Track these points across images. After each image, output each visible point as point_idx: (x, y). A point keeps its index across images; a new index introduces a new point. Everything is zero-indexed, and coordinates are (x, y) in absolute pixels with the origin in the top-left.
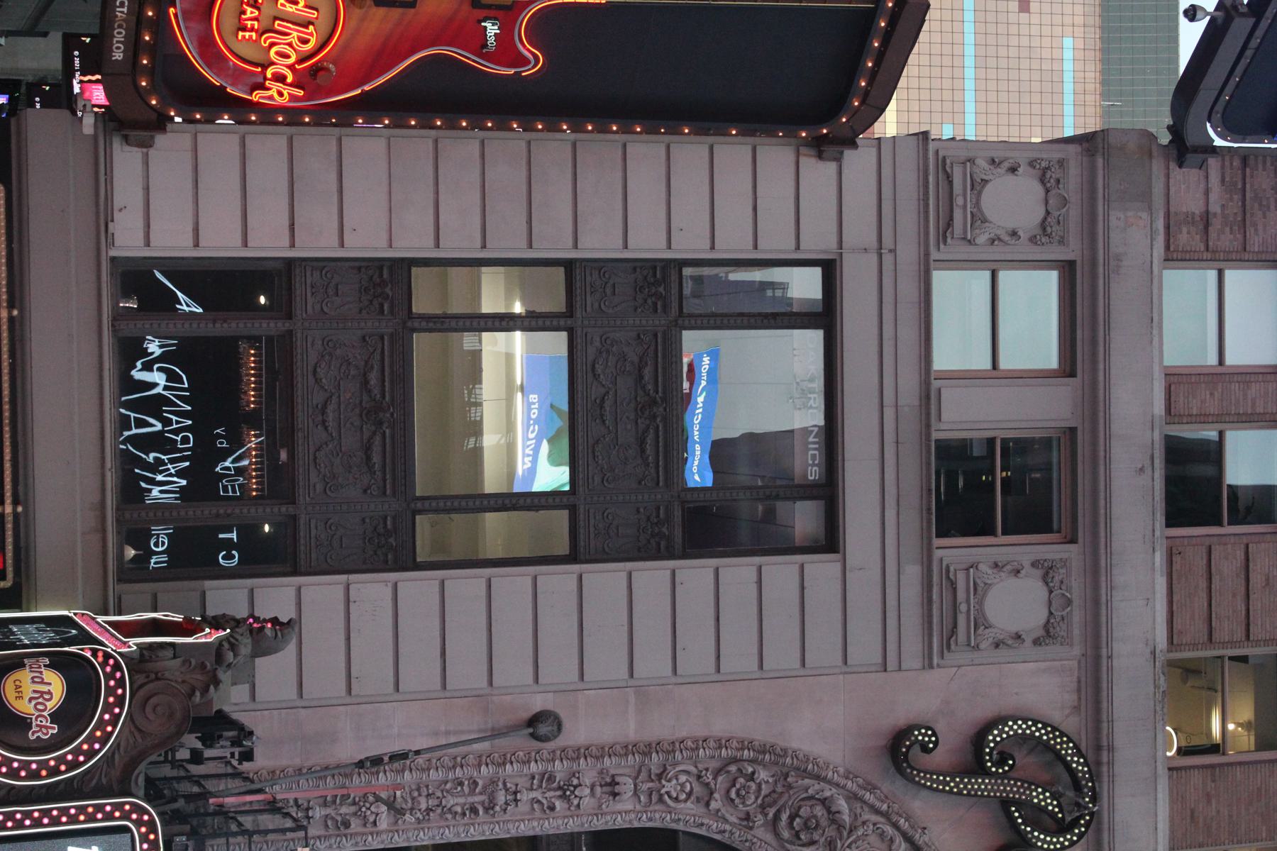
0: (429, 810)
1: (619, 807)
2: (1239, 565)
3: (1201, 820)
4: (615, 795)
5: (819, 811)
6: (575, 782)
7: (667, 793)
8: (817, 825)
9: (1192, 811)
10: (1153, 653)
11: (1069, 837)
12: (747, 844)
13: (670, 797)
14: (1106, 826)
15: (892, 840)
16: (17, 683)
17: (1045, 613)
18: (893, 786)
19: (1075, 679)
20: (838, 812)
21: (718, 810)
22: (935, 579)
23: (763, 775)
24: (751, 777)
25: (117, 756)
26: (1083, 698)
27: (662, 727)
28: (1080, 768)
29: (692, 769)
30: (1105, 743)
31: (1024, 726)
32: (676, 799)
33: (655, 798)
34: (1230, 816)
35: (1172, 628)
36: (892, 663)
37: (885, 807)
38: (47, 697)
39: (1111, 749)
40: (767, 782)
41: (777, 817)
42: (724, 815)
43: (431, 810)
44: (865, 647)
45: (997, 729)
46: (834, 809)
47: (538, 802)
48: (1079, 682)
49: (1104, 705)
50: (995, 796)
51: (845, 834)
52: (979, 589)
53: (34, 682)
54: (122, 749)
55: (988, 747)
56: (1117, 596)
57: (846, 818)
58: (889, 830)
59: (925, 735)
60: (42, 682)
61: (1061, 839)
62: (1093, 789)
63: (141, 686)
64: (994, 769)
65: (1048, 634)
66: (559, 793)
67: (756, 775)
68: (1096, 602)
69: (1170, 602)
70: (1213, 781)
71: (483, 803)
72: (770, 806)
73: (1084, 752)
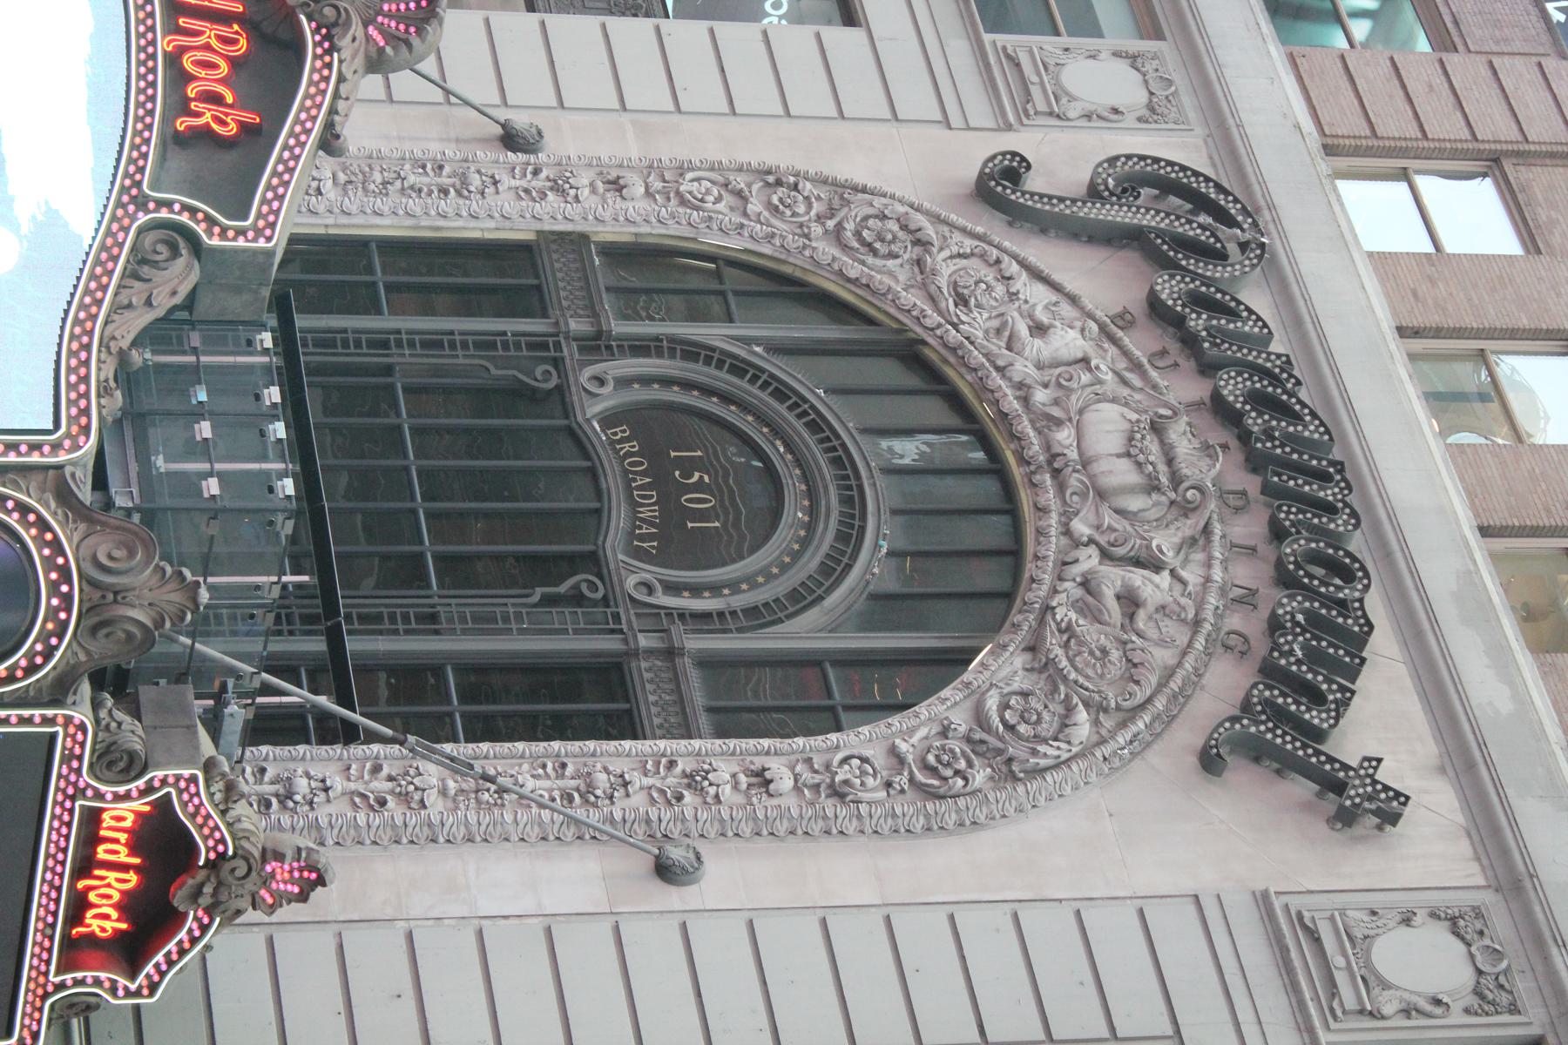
0: (385, 183)
1: (630, 205)
2: (1386, 70)
3: (1430, 301)
4: (620, 189)
5: (894, 227)
6: (568, 174)
7: (690, 193)
8: (895, 237)
10: (1298, 127)
12: (807, 253)
13: (695, 198)
14: (1291, 279)
15: (998, 261)
17: (1145, 94)
18: (989, 224)
19: (1205, 155)
20: (920, 230)
21: (759, 214)
22: (992, 59)
23: (807, 187)
24: (795, 187)
27: (669, 150)
30: (1262, 203)
32: (702, 200)
33: (674, 202)
34: (1470, 300)
35: (1319, 122)
36: (956, 120)
37: (979, 229)
39: (1272, 207)
40: (819, 198)
41: (840, 227)
42: (767, 220)
43: (388, 183)
44: (916, 98)
46: (912, 227)
47: (527, 191)
48: (1211, 158)
49: (1249, 170)
51: (935, 250)
52: (1051, 68)
56: (1229, 73)
57: (930, 231)
58: (995, 252)
65: (1152, 113)
66: (549, 184)
67: (800, 187)
68: (1207, 84)
69: (1308, 99)
70: (1433, 265)
71: (453, 186)
72: (832, 217)
73: (1226, 185)
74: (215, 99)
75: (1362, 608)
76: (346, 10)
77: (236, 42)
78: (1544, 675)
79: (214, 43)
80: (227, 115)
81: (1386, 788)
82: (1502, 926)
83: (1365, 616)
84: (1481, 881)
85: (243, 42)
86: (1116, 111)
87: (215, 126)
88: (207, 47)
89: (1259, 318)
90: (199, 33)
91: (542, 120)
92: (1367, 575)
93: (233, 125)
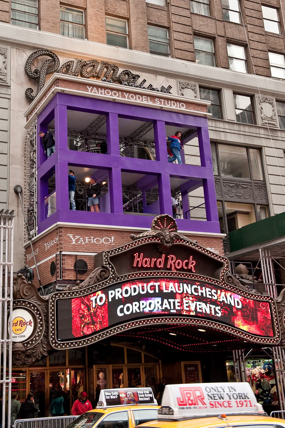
9: (51, 27)
11: (56, 59)
16: (16, 330)
25: (38, 303)
26: (20, 48)
28: (40, 53)
29: (32, 153)
31: (28, 65)
38: (21, 322)
45: (28, 72)
50: (45, 76)
53: (17, 326)
54: (37, 302)
55: (32, 75)
59: (28, 91)
60: (17, 323)
61: (57, 61)
62: (45, 51)
63: (21, 296)
64: (38, 75)
74: (187, 264)
75: (134, 75)
76: (174, 235)
77: (172, 257)
78: (136, 50)
79: (173, 262)
80: (191, 262)
81: (168, 88)
82: (182, 81)
83: (136, 75)
84: (175, 80)
85: (173, 256)
86: (4, 62)
87: (193, 265)
88: (174, 263)
89: (70, 61)
90: (171, 264)
91: (12, 185)
92: (128, 71)
93: (193, 261)
